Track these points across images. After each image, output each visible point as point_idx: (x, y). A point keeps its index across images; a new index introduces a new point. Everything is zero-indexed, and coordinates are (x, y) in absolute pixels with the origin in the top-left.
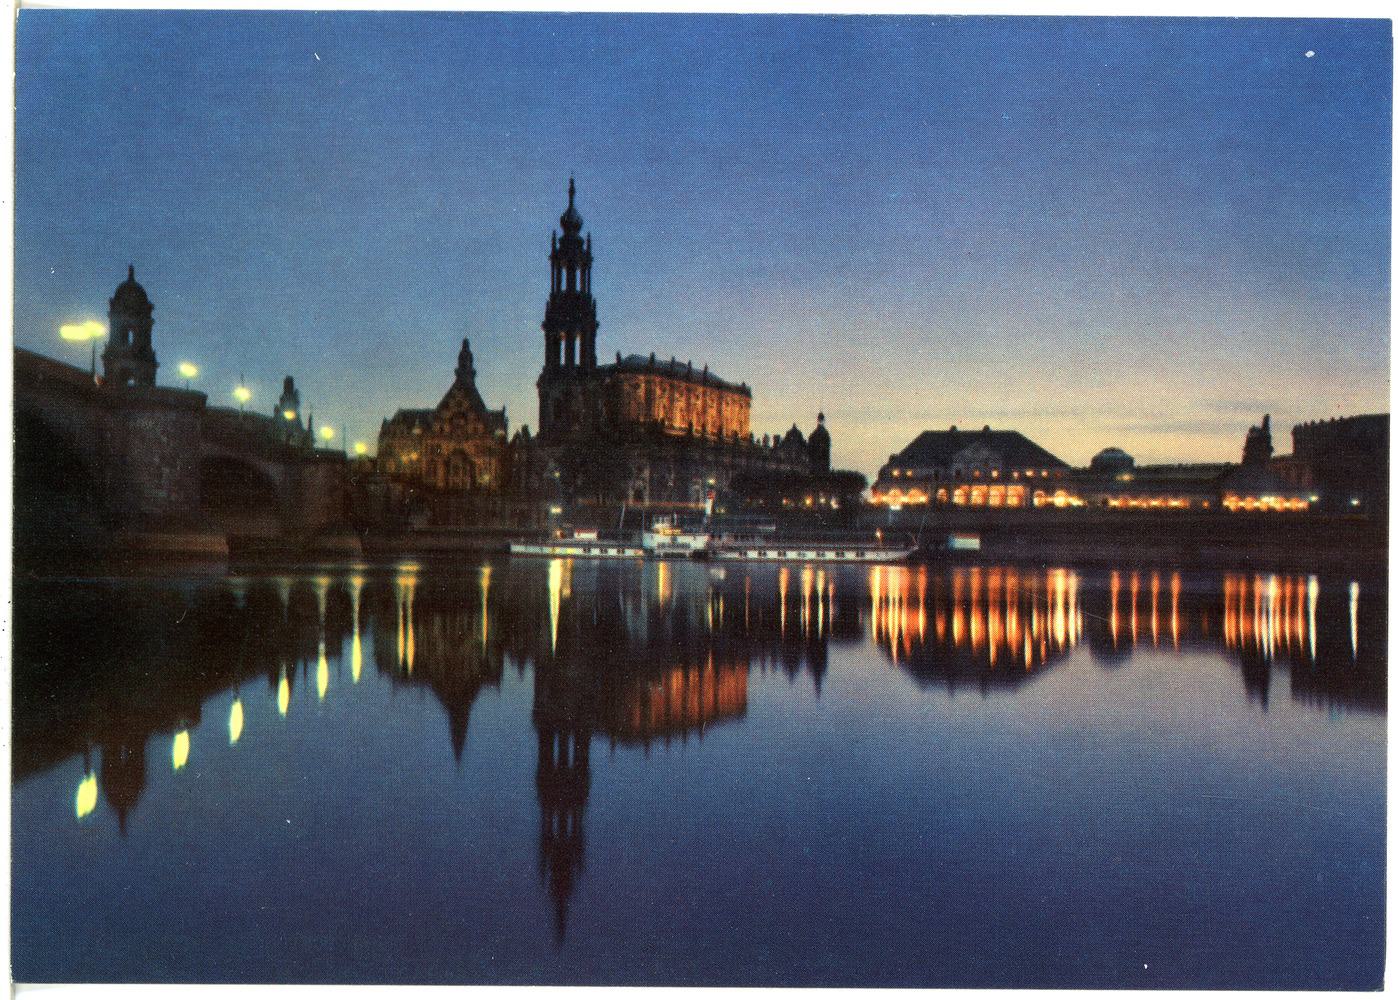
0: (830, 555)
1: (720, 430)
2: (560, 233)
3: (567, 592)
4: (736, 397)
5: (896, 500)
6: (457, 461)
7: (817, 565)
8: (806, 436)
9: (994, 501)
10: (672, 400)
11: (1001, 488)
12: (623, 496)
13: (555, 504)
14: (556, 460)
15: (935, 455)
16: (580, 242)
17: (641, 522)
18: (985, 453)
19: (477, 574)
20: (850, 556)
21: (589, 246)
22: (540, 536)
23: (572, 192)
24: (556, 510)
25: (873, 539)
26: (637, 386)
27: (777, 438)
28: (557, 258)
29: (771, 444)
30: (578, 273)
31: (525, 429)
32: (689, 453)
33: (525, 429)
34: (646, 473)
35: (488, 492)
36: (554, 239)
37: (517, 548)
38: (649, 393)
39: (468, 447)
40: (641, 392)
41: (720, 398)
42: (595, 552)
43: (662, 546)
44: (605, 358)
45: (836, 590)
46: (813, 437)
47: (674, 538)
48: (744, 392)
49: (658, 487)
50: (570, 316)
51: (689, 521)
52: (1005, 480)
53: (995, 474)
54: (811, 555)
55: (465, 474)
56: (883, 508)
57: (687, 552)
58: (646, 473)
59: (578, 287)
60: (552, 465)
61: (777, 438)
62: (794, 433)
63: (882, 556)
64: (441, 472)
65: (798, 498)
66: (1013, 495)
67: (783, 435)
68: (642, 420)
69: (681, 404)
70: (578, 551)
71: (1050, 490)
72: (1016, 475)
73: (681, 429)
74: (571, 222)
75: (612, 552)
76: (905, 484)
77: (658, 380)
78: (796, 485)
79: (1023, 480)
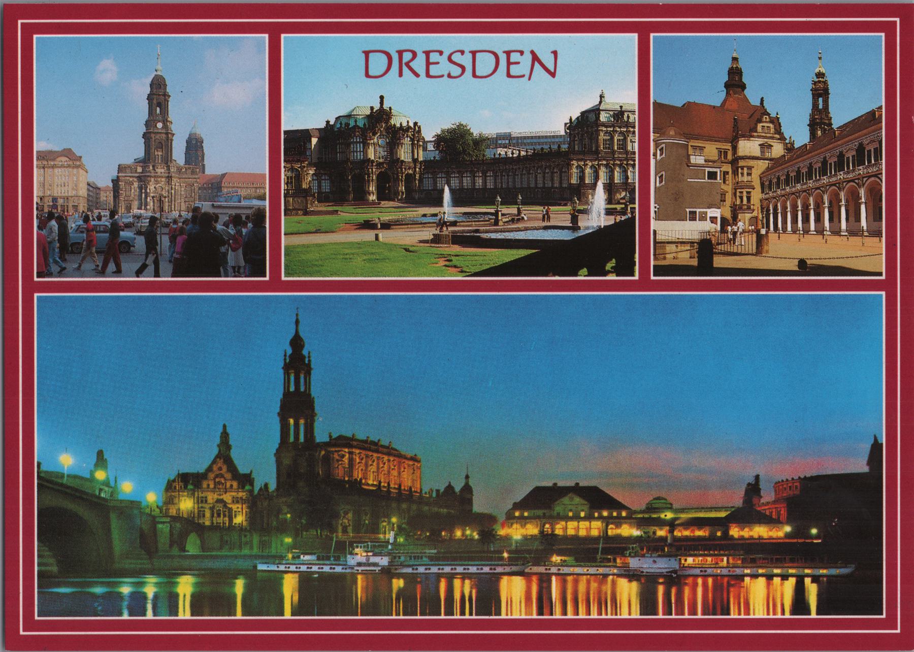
0: (473, 569)
1: (400, 486)
2: (289, 351)
3: (296, 598)
4: (411, 463)
5: (517, 533)
6: (219, 507)
7: (464, 576)
8: (457, 489)
9: (582, 533)
10: (366, 465)
11: (587, 523)
12: (333, 530)
13: (288, 536)
14: (288, 506)
15: (543, 500)
16: (304, 357)
17: (344, 548)
18: (577, 500)
19: (233, 585)
20: (486, 569)
21: (309, 361)
22: (280, 558)
23: (297, 322)
24: (288, 540)
25: (502, 559)
26: (343, 456)
27: (438, 491)
28: (287, 368)
29: (434, 495)
30: (302, 376)
31: (266, 485)
32: (382, 500)
33: (266, 485)
34: (350, 515)
35: (241, 528)
36: (285, 355)
37: (261, 567)
38: (351, 460)
39: (227, 497)
40: (346, 460)
41: (400, 463)
42: (315, 568)
43: (359, 564)
44: (321, 436)
45: (477, 593)
46: (462, 490)
47: (368, 560)
48: (414, 459)
49: (357, 527)
50: (297, 404)
51: (378, 548)
52: (589, 518)
53: (582, 514)
54: (460, 569)
55: (224, 516)
56: (507, 538)
57: (377, 569)
58: (350, 515)
59: (302, 389)
60: (285, 509)
61: (438, 491)
62: (450, 488)
63: (507, 569)
64: (208, 514)
65: (452, 532)
66: (595, 528)
67: (442, 490)
68: (347, 479)
69: (373, 468)
70: (304, 568)
71: (618, 526)
72: (596, 515)
73: (373, 485)
74: (297, 342)
75: (326, 569)
76: (523, 520)
77: (358, 451)
78: (451, 523)
79: (601, 518)
